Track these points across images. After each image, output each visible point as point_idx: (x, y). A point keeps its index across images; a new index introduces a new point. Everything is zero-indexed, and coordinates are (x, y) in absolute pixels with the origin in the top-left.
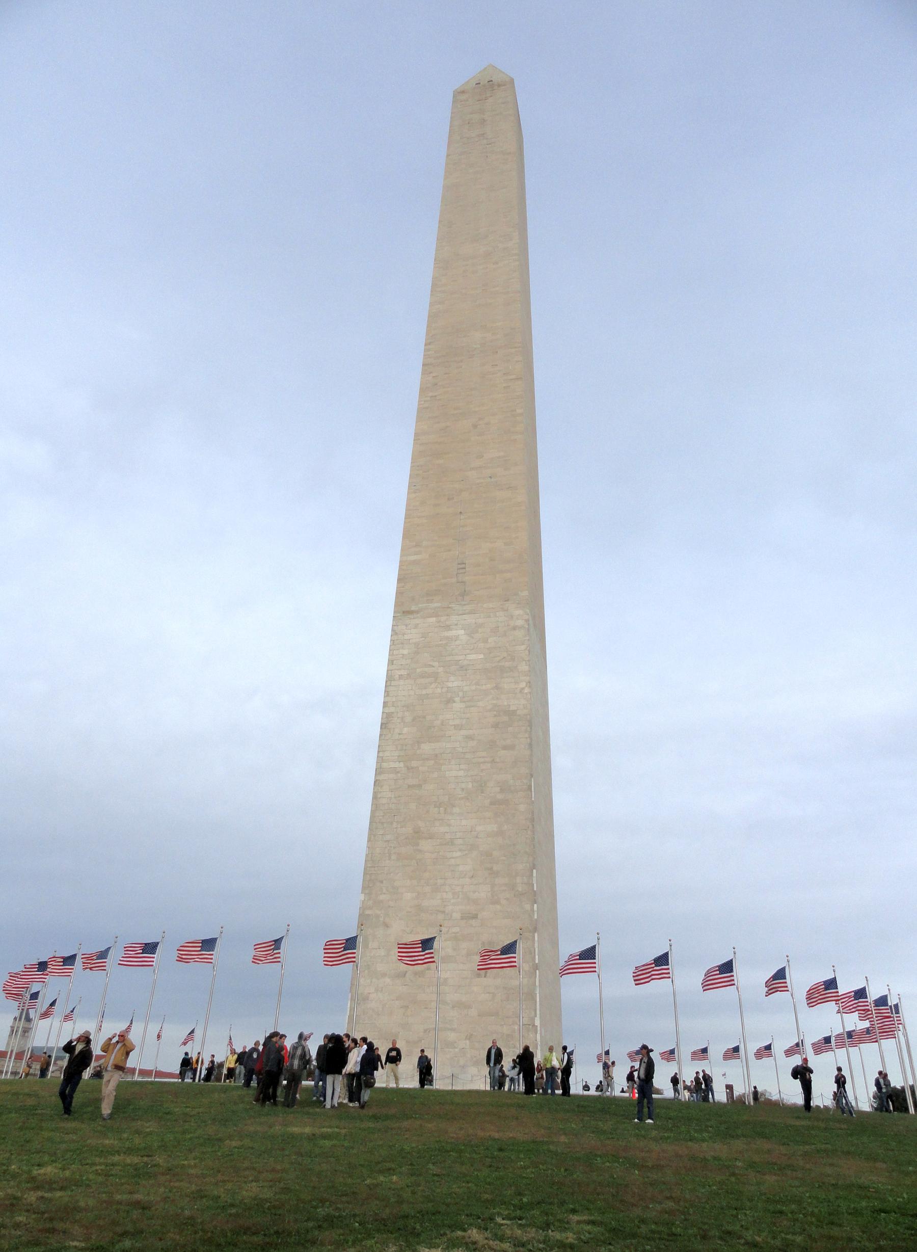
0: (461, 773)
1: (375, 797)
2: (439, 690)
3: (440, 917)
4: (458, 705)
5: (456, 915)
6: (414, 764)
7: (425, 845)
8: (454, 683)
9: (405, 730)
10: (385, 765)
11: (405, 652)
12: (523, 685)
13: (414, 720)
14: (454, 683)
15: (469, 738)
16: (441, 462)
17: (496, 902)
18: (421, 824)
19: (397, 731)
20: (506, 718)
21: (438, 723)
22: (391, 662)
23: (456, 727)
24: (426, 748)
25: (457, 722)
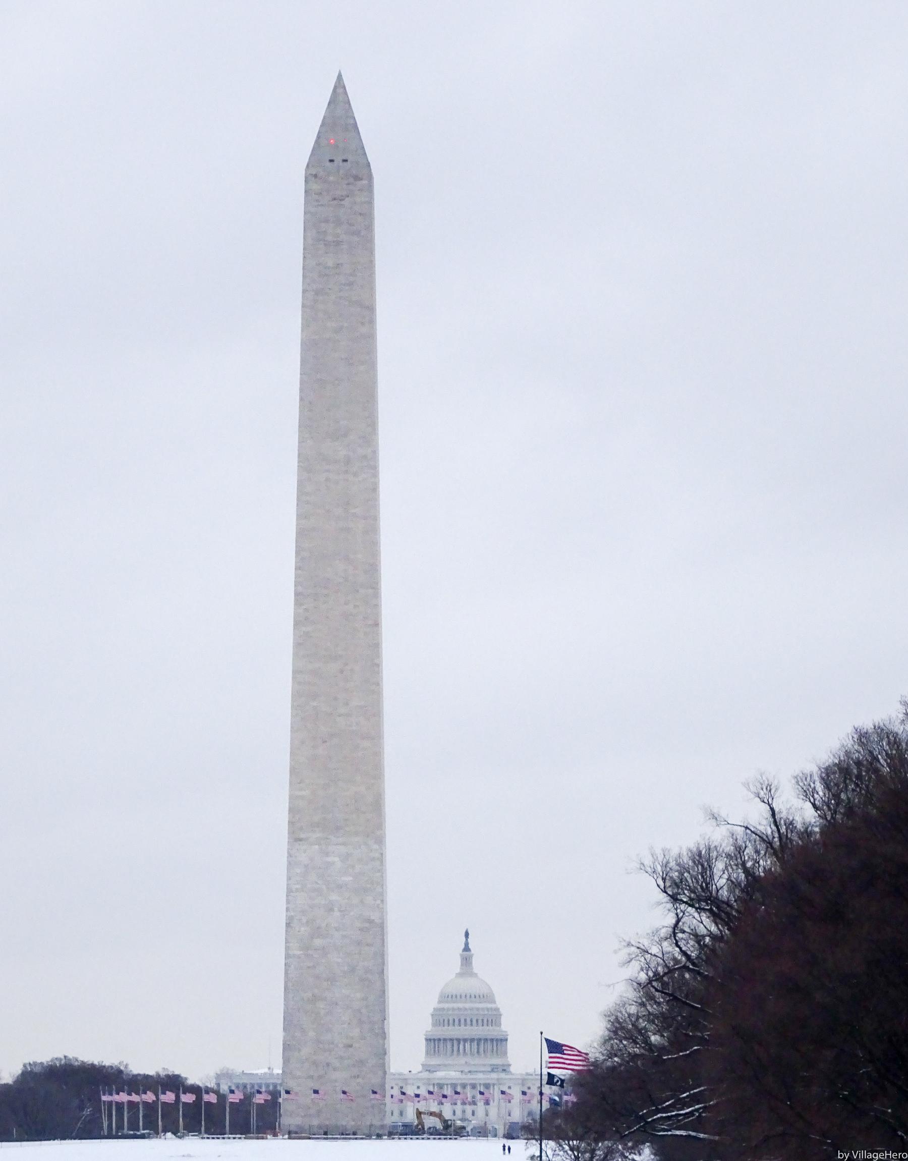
0: (340, 960)
1: (286, 973)
2: (323, 902)
3: (331, 1046)
4: (337, 914)
5: (341, 1045)
6: (310, 952)
7: (321, 1005)
8: (334, 897)
9: (303, 929)
10: (291, 952)
11: (298, 871)
12: (379, 902)
13: (307, 922)
14: (334, 897)
15: (344, 937)
16: (315, 704)
17: (364, 1038)
18: (316, 991)
19: (297, 929)
20: (367, 925)
21: (324, 925)
22: (289, 878)
23: (337, 929)
24: (318, 942)
25: (336, 925)
